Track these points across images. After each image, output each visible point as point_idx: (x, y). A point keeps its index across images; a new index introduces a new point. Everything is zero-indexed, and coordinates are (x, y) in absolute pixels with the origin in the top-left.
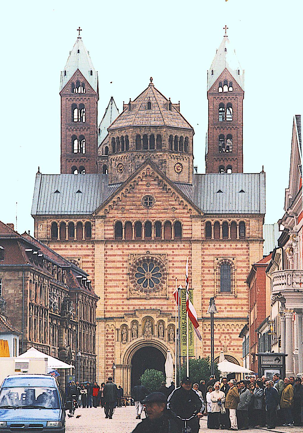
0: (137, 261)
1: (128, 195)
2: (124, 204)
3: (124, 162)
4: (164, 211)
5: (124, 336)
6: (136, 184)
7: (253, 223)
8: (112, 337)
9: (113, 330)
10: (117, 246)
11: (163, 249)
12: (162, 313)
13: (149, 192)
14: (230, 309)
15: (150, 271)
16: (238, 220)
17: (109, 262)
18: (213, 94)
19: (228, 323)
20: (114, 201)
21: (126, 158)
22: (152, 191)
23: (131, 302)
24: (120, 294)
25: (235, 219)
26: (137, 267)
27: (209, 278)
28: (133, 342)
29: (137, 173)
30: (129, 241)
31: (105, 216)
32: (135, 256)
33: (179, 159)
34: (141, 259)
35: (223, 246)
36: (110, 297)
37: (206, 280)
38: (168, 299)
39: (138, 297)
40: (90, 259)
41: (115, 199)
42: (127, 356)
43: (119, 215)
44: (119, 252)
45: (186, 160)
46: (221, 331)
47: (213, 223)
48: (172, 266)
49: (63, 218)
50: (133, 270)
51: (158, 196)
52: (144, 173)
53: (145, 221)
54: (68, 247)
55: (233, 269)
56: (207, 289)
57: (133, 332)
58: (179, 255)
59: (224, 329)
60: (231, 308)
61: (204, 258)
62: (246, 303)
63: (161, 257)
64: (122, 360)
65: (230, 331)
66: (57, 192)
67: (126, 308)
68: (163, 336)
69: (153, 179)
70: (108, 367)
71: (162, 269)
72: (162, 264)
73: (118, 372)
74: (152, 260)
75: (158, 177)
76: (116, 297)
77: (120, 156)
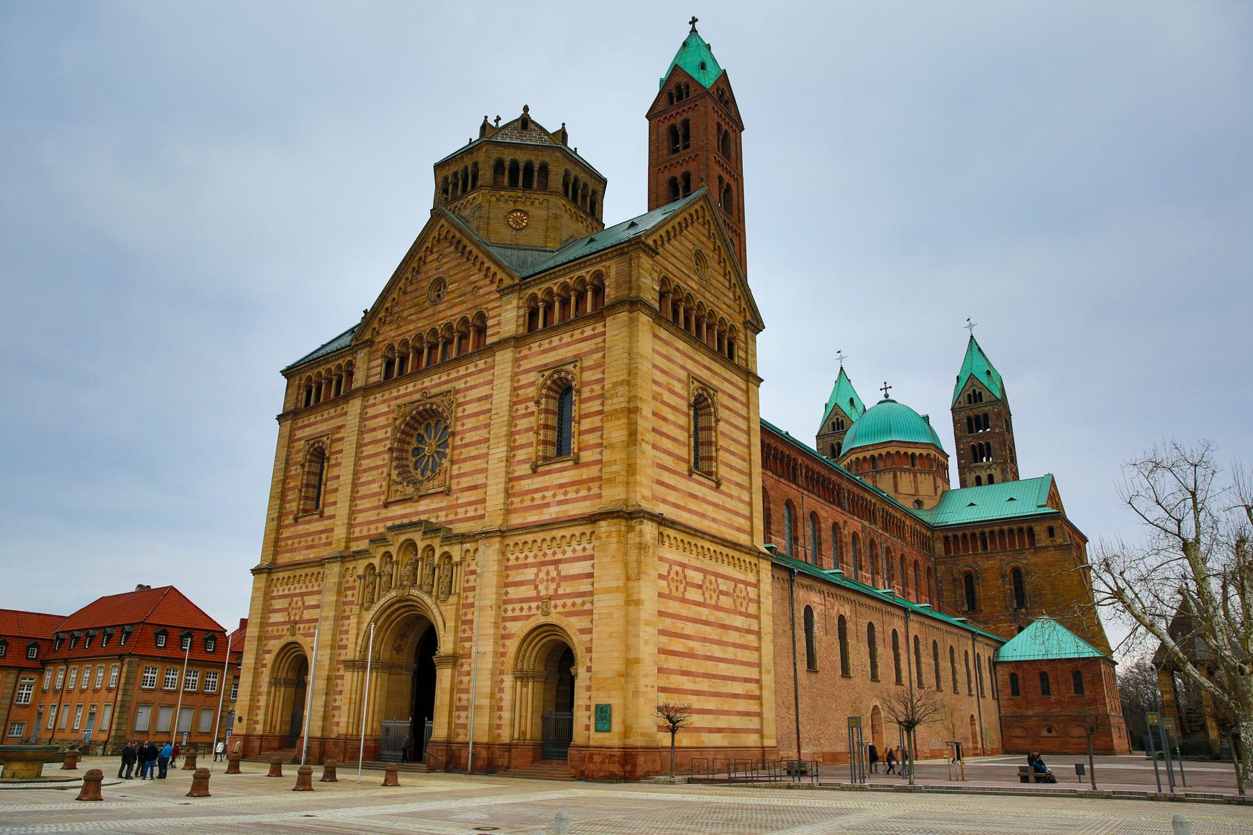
0: (408, 418)
9: (355, 581)
10: (383, 396)
12: (431, 529)
19: (554, 533)
20: (387, 309)
22: (445, 267)
25: (582, 273)
26: (416, 433)
31: (373, 342)
33: (518, 203)
34: (414, 412)
37: (519, 432)
38: (448, 495)
43: (393, 334)
44: (383, 408)
45: (541, 204)
46: (540, 559)
50: (400, 441)
56: (521, 454)
58: (475, 387)
59: (548, 551)
64: (358, 648)
65: (559, 556)
68: (433, 585)
70: (340, 666)
76: (368, 505)
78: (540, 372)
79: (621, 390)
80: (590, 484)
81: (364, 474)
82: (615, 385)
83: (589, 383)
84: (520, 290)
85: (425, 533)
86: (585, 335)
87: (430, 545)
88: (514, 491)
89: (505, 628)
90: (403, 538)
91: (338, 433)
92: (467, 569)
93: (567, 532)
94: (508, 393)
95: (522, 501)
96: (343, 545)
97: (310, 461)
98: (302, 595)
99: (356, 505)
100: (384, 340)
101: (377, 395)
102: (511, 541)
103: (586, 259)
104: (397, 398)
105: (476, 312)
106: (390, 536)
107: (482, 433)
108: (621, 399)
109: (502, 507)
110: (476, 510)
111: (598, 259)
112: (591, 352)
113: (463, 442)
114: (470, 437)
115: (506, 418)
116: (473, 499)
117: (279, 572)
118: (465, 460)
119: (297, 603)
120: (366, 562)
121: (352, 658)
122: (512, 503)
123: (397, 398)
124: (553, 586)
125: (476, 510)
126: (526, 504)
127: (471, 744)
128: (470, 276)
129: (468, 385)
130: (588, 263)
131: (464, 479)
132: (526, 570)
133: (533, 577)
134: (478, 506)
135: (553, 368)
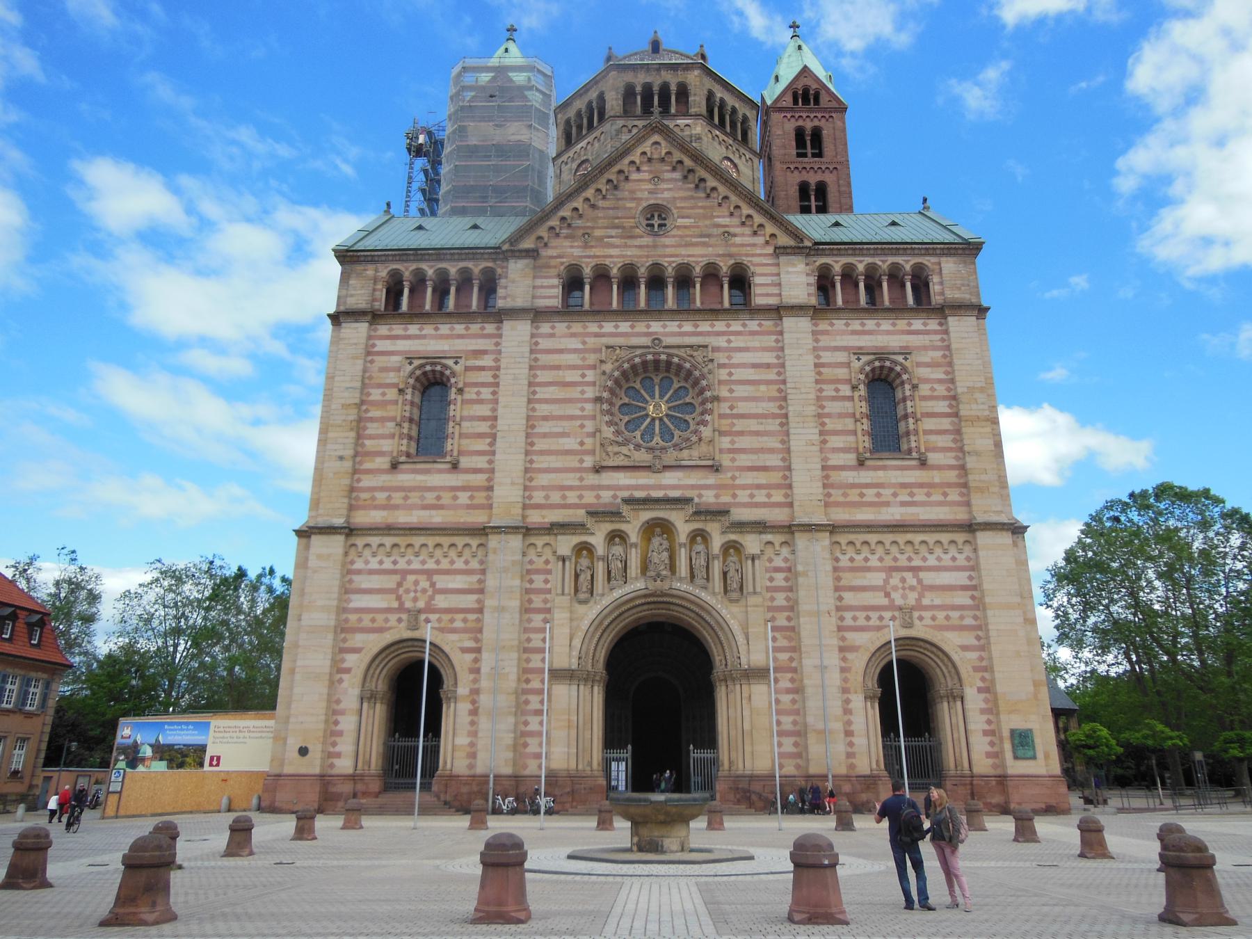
0: (626, 366)
1: (601, 203)
2: (589, 224)
3: (592, 155)
4: (699, 240)
5: (582, 578)
6: (622, 178)
7: (949, 266)
8: (546, 581)
9: (547, 562)
10: (569, 328)
11: (701, 334)
13: (659, 196)
14: (908, 499)
15: (661, 397)
16: (907, 261)
17: (544, 368)
18: (781, 110)
19: (909, 537)
20: (563, 219)
21: (599, 140)
22: (666, 195)
23: (608, 478)
24: (573, 457)
25: (899, 260)
26: (625, 386)
27: (838, 410)
28: (607, 598)
29: (626, 152)
30: (601, 313)
31: (538, 254)
32: (618, 351)
34: (637, 360)
35: (870, 324)
36: (545, 465)
38: (717, 470)
39: (626, 463)
40: (487, 361)
41: (565, 212)
42: (590, 641)
43: (577, 252)
44: (575, 344)
46: (889, 562)
47: (837, 268)
48: (728, 378)
49: (421, 260)
50: (612, 392)
51: (682, 205)
52: (644, 153)
53: (648, 264)
54: (428, 330)
55: (907, 387)
56: (836, 442)
57: (612, 566)
59: (898, 556)
60: (912, 495)
61: (818, 357)
62: (955, 480)
63: (695, 354)
64: (575, 653)
65: (917, 562)
66: (420, 228)
67: (589, 498)
68: (708, 579)
69: (669, 168)
70: (530, 676)
71: (697, 390)
72: (697, 373)
73: (564, 694)
74: (669, 363)
75: (680, 162)
76: (559, 465)
77: (583, 144)
78: (855, 354)
79: (978, 395)
80: (946, 490)
81: (541, 423)
82: (971, 390)
83: (927, 381)
84: (808, 255)
85: (697, 513)
86: (913, 328)
87: (703, 530)
88: (831, 481)
89: (843, 639)
90: (646, 515)
91: (476, 359)
92: (768, 565)
93: (931, 538)
94: (812, 367)
95: (845, 495)
96: (518, 510)
97: (414, 388)
98: (429, 573)
99: (531, 462)
100: (559, 257)
101: (556, 324)
102: (843, 539)
103: (909, 246)
104: (597, 335)
105: (732, 262)
106: (625, 510)
107: (772, 407)
108: (982, 407)
109: (821, 497)
110: (769, 496)
111: (923, 252)
112: (925, 348)
113: (735, 411)
114: (743, 408)
115: (812, 396)
116: (764, 482)
117: (370, 535)
118: (741, 433)
119: (416, 583)
120: (576, 539)
121: (565, 665)
122: (829, 495)
123: (597, 335)
124: (912, 598)
125: (769, 496)
126: (848, 499)
127: (830, 777)
128: (712, 217)
129: (732, 345)
130: (909, 252)
131: (743, 456)
132: (869, 575)
133: (881, 583)
134: (773, 492)
135: (874, 354)
